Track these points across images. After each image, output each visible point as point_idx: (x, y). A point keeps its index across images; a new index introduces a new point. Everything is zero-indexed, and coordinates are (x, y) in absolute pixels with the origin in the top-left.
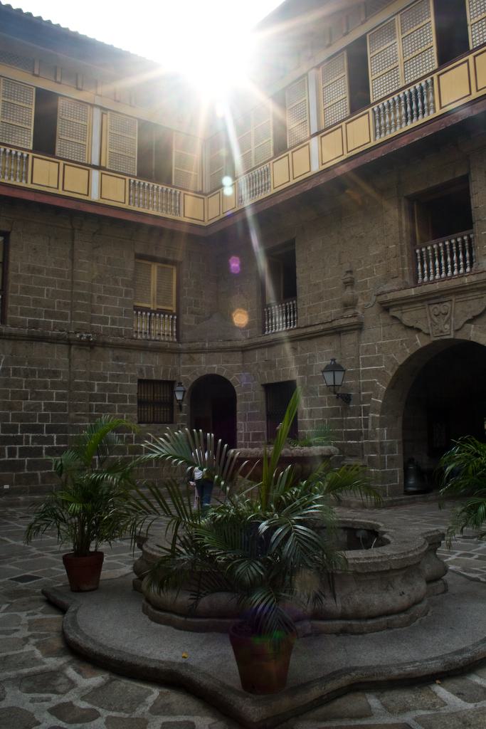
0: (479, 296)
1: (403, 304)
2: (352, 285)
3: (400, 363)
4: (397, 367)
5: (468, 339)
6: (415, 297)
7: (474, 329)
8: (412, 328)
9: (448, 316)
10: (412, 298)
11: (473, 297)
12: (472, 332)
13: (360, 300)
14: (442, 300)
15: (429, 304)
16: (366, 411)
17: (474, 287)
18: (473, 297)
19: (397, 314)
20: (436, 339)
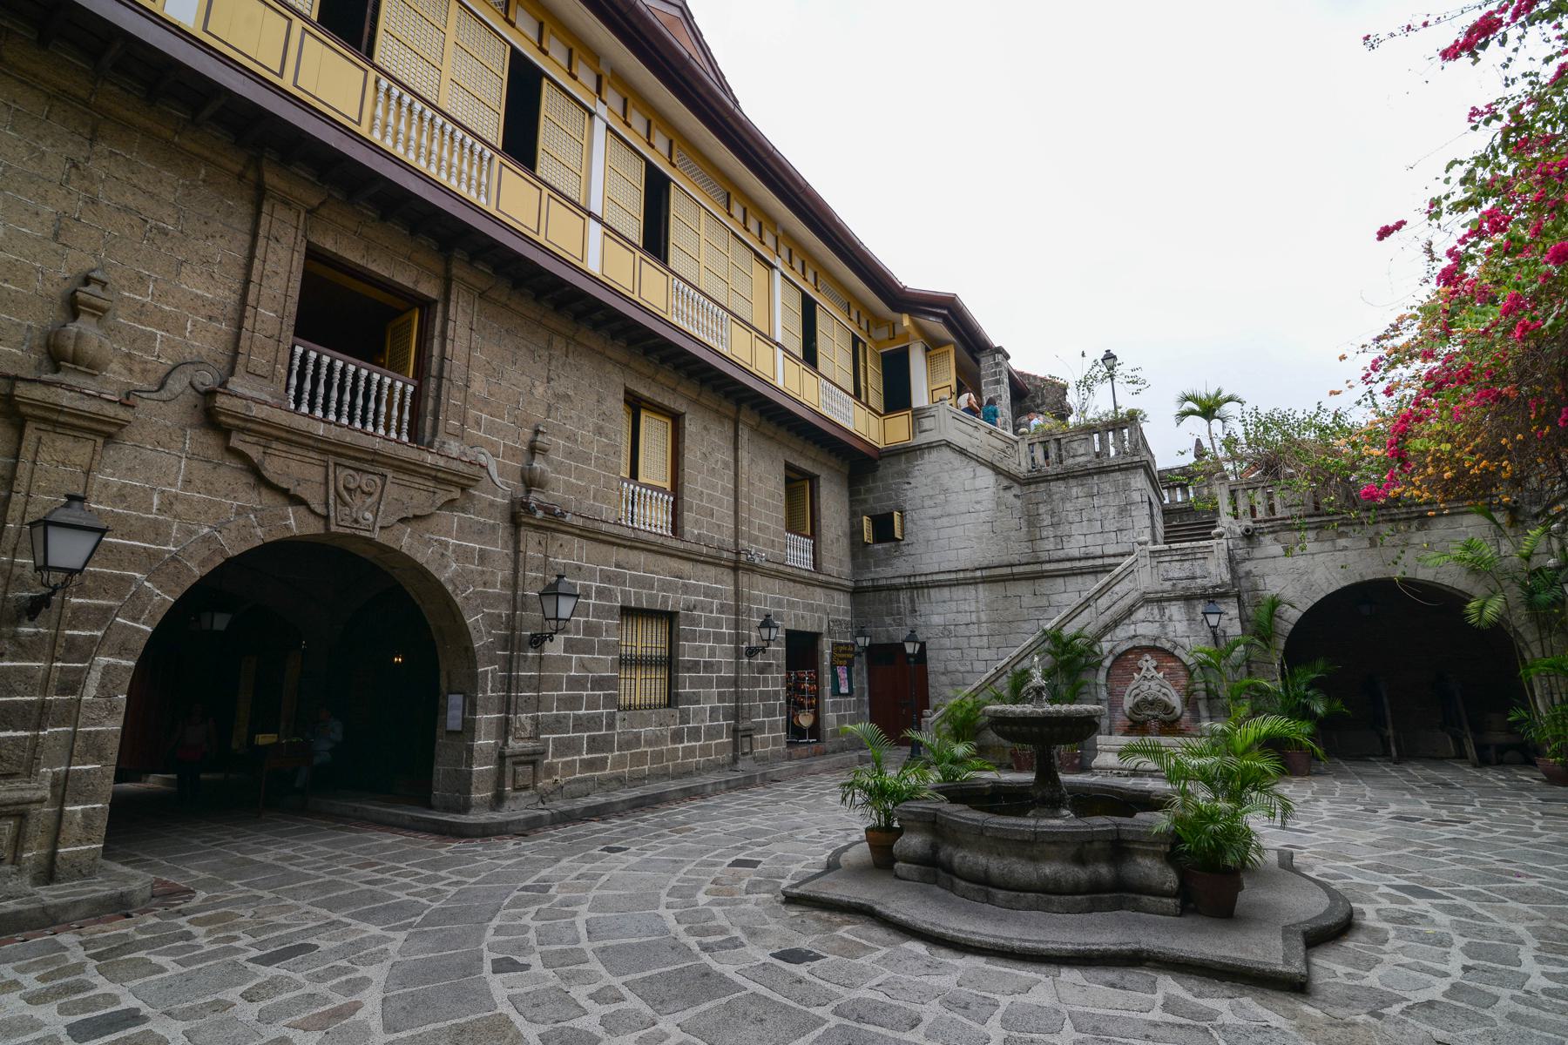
1: (277, 439)
2: (100, 317)
3: (231, 554)
4: (219, 560)
6: (316, 440)
7: (411, 536)
8: (284, 492)
10: (310, 438)
13: (115, 366)
16: (83, 650)
19: (255, 453)
20: (341, 530)
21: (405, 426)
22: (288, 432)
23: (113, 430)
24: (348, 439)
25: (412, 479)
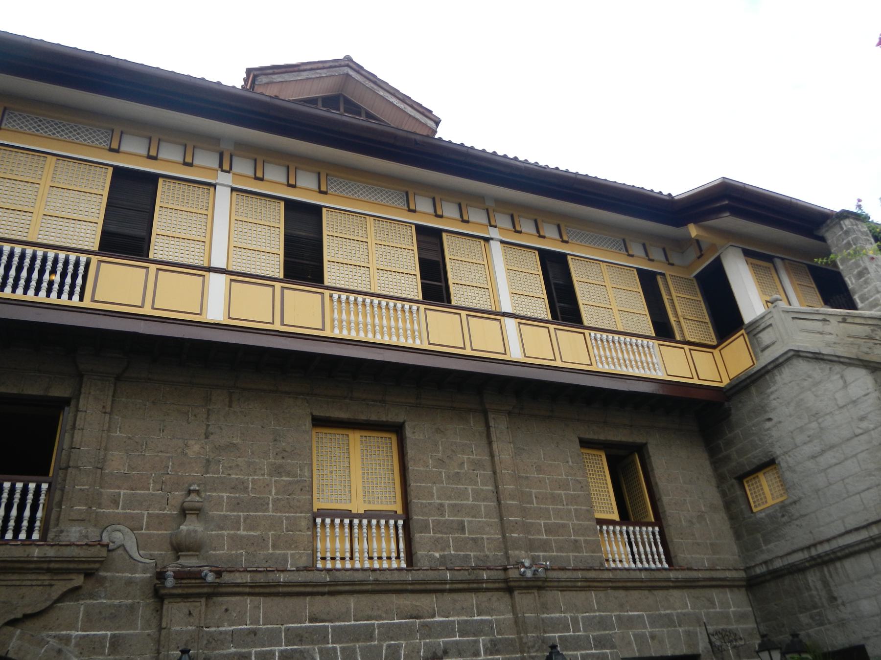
0: (47, 583)
11: (34, 583)
17: (45, 566)
18: (34, 583)
21: (38, 524)
25: (22, 577)
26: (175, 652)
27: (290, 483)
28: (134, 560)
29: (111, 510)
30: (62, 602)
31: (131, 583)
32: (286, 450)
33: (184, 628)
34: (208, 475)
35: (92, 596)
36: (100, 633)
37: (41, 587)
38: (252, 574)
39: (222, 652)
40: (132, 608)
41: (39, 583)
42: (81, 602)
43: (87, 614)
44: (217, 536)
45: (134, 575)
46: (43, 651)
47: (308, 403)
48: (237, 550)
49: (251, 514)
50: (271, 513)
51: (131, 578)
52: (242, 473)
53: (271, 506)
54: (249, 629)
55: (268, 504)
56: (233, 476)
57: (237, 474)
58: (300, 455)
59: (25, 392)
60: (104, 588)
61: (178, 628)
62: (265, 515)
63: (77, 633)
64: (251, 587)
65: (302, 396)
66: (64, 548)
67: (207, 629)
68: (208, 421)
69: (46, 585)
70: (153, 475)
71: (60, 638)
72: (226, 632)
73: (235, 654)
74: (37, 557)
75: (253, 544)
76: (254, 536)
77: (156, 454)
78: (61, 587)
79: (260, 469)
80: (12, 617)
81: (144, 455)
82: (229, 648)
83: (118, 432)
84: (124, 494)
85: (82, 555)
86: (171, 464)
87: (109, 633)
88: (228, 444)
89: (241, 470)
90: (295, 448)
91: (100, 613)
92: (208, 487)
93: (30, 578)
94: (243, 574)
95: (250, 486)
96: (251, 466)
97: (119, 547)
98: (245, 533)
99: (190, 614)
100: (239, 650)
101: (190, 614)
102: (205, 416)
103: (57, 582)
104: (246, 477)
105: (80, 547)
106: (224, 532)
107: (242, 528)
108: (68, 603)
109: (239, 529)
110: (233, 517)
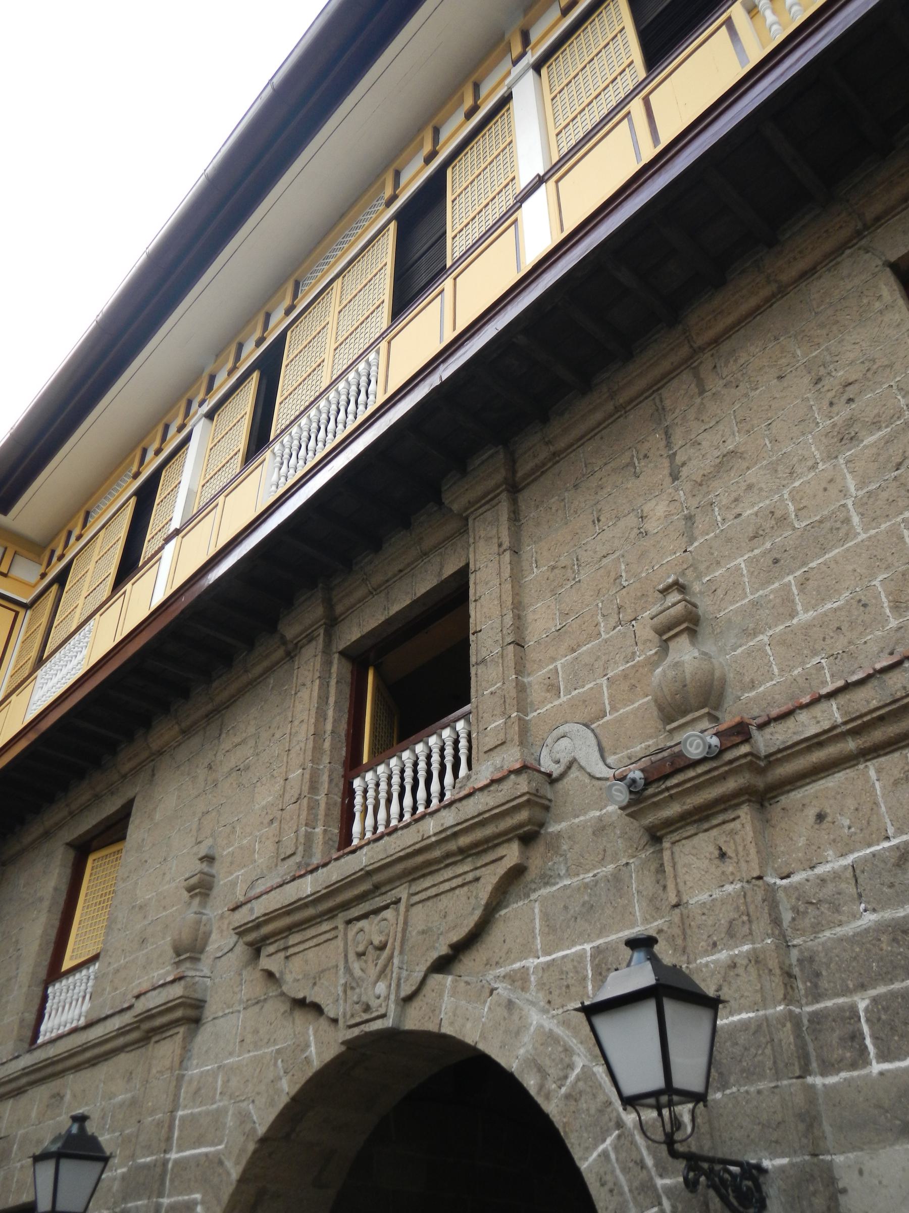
0: (470, 877)
1: (290, 929)
5: (431, 1027)
9: (387, 952)
10: (306, 905)
12: (447, 1003)
14: (378, 902)
15: (349, 922)
17: (452, 846)
22: (288, 913)
23: (190, 1013)
24: (334, 878)
26: (709, 959)
27: (888, 441)
28: (599, 779)
29: (549, 706)
30: (506, 907)
31: (603, 828)
32: (850, 381)
33: (717, 894)
34: (696, 544)
35: (546, 879)
36: (574, 950)
37: (466, 889)
38: (842, 699)
39: (840, 931)
40: (617, 880)
41: (459, 881)
42: (534, 896)
43: (546, 916)
44: (749, 653)
45: (604, 811)
46: (486, 1010)
47: (867, 252)
48: (803, 663)
49: (813, 565)
50: (863, 536)
51: (600, 818)
52: (764, 494)
53: (856, 519)
54: (897, 847)
55: (847, 520)
56: (749, 512)
57: (753, 505)
58: (891, 366)
59: (418, 595)
60: (561, 856)
61: (704, 897)
62: (848, 550)
63: (536, 961)
64: (855, 732)
65: (848, 252)
66: (464, 802)
67: (785, 882)
68: (670, 449)
69: (470, 882)
70: (600, 605)
71: (510, 978)
72: (836, 876)
73: (881, 928)
74: (435, 835)
75: (839, 628)
76: (835, 610)
77: (597, 566)
78: (491, 877)
79: (804, 459)
80: (435, 955)
81: (579, 581)
82: (855, 916)
83: (535, 570)
84: (563, 666)
85: (492, 804)
86: (623, 567)
87: (588, 947)
88: (718, 461)
89: (761, 489)
90: (874, 361)
91: (566, 908)
92: (702, 567)
93: (446, 877)
94: (817, 710)
95: (791, 508)
96: (780, 468)
97: (569, 767)
98: (811, 614)
99: (723, 855)
100: (888, 914)
101: (723, 855)
102: (663, 443)
103: (483, 869)
104: (776, 497)
105: (486, 792)
106: (761, 637)
107: (799, 608)
108: (515, 906)
109: (793, 614)
110: (772, 597)
